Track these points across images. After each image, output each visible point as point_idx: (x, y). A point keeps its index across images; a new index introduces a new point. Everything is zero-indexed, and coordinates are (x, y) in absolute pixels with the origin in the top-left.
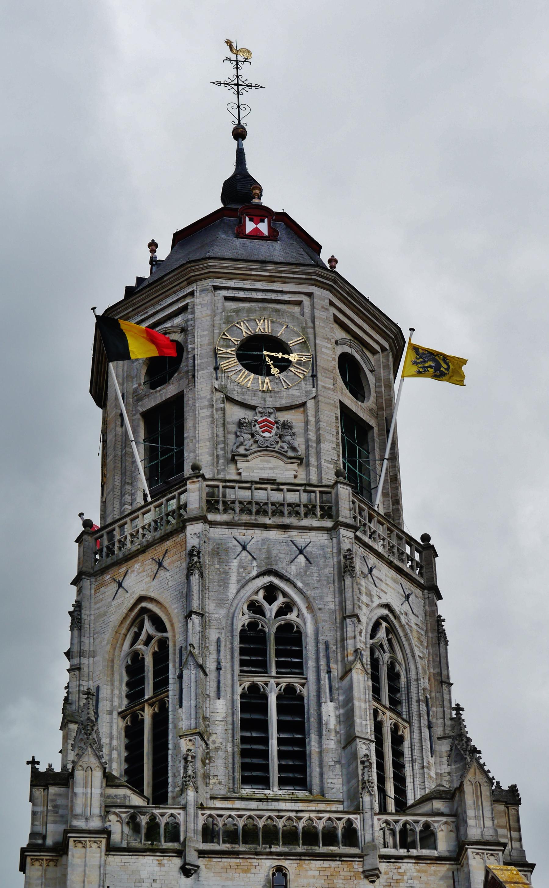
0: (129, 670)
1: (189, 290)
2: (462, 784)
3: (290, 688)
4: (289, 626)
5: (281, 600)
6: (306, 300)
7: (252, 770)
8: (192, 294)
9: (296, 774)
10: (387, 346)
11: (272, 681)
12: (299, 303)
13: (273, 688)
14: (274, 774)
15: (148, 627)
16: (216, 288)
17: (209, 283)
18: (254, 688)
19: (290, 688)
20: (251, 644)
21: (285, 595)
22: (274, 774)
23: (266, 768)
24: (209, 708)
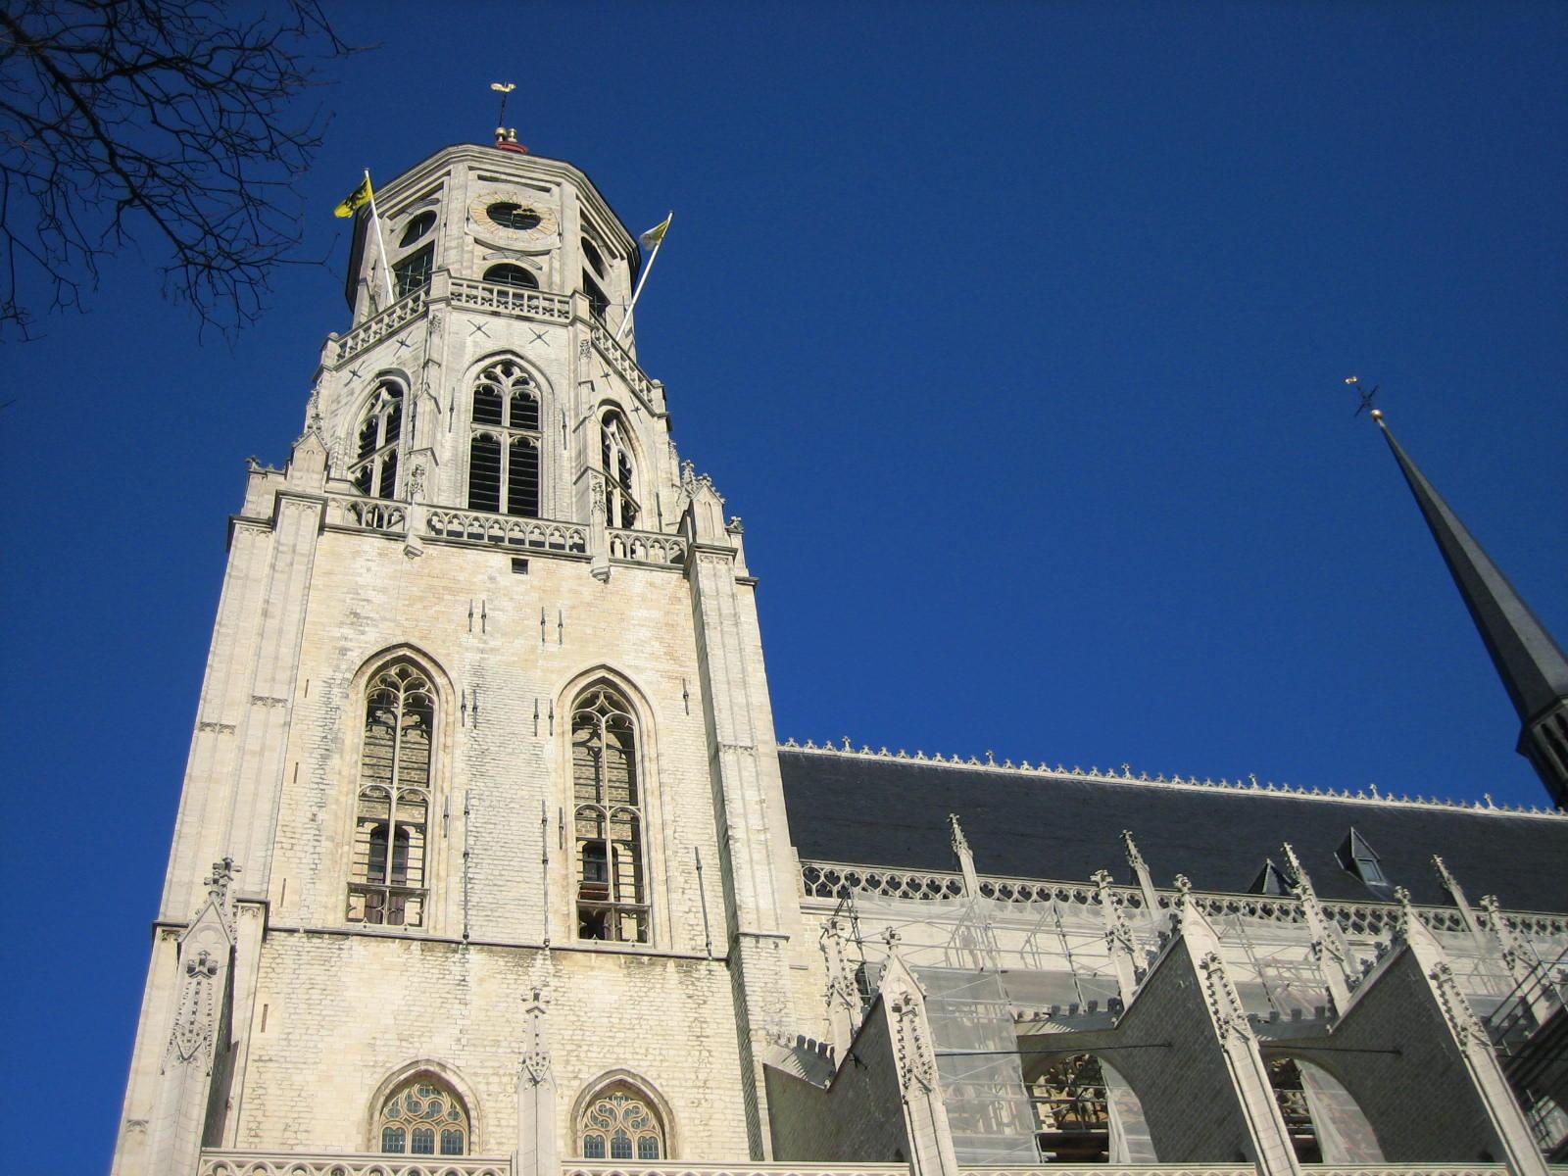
0: (363, 436)
1: (447, 169)
2: (691, 504)
3: (523, 442)
4: (525, 397)
5: (517, 373)
6: (554, 188)
7: (482, 496)
8: (448, 173)
9: (526, 502)
10: (625, 255)
11: (506, 431)
12: (547, 190)
13: (505, 436)
14: (504, 506)
15: (385, 394)
16: (471, 168)
17: (467, 164)
18: (486, 438)
19: (523, 442)
20: (486, 406)
21: (522, 369)
22: (504, 506)
23: (497, 499)
24: (442, 442)
